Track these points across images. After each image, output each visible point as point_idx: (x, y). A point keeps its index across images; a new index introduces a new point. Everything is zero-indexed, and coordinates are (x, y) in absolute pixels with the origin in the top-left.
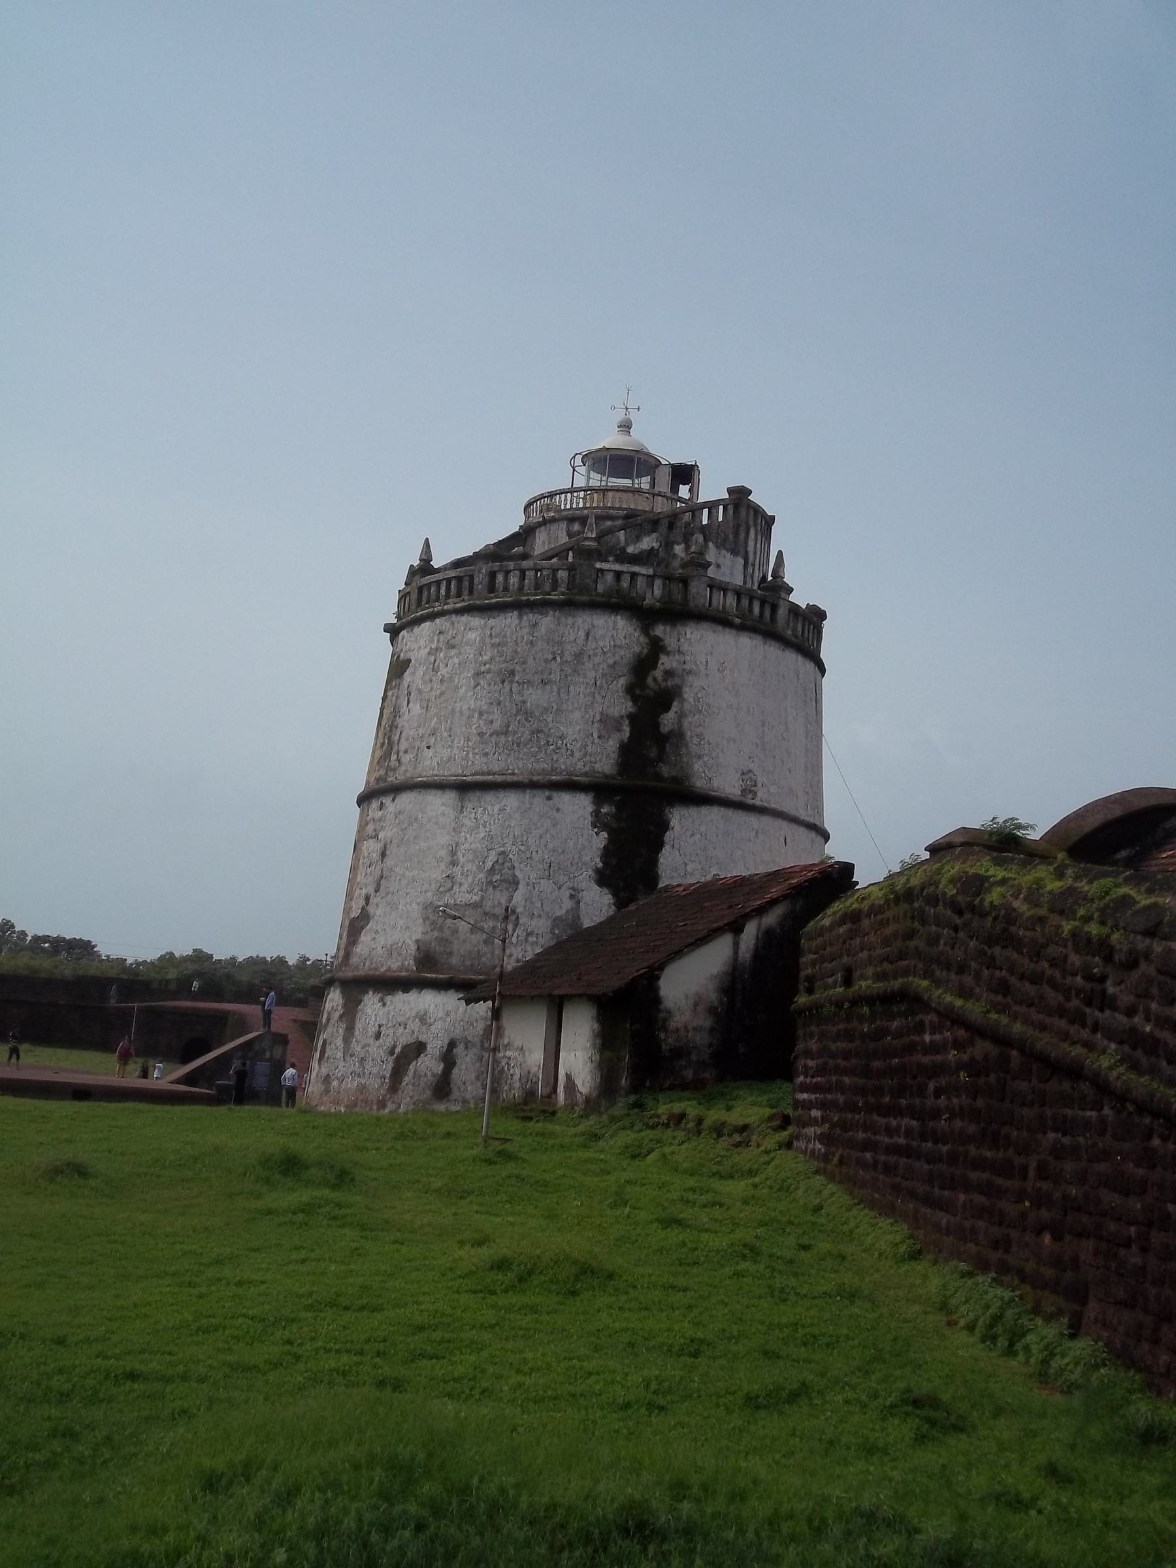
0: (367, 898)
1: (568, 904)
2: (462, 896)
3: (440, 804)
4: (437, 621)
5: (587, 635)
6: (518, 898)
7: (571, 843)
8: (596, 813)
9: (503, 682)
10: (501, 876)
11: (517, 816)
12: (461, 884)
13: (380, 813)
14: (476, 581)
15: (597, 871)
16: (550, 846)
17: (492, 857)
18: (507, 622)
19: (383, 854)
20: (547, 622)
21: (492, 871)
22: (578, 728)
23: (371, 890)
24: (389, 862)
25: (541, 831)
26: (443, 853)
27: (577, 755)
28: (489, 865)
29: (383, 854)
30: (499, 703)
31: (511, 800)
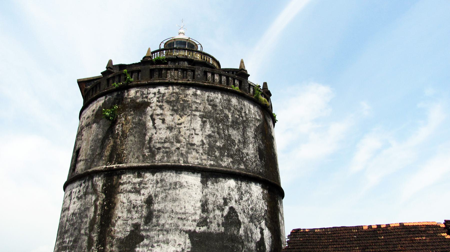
0: (136, 226)
1: (260, 236)
2: (214, 228)
3: (194, 180)
4: (171, 88)
5: (249, 111)
6: (241, 232)
7: (258, 206)
8: (263, 192)
9: (218, 124)
10: (232, 219)
11: (236, 190)
12: (211, 222)
13: (139, 180)
14: (196, 73)
15: (266, 219)
16: (251, 207)
17: (227, 209)
18: (218, 97)
19: (149, 201)
20: (234, 101)
21: (227, 218)
22: (252, 152)
23: (142, 221)
24: (156, 207)
25: (246, 198)
26: (199, 204)
27: (254, 164)
28: (225, 213)
29: (149, 201)
30: (219, 133)
31: (232, 183)
